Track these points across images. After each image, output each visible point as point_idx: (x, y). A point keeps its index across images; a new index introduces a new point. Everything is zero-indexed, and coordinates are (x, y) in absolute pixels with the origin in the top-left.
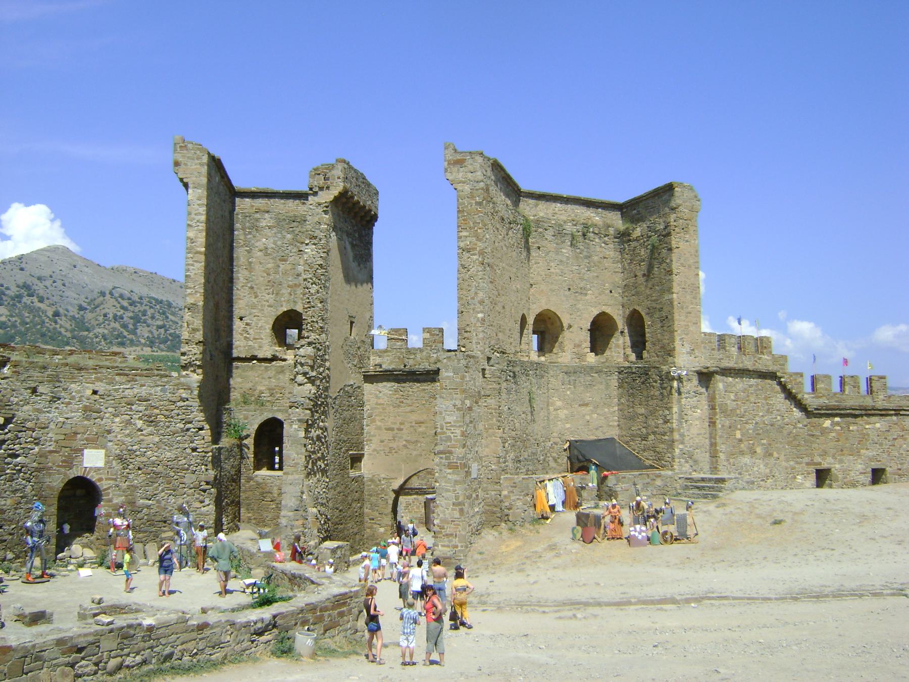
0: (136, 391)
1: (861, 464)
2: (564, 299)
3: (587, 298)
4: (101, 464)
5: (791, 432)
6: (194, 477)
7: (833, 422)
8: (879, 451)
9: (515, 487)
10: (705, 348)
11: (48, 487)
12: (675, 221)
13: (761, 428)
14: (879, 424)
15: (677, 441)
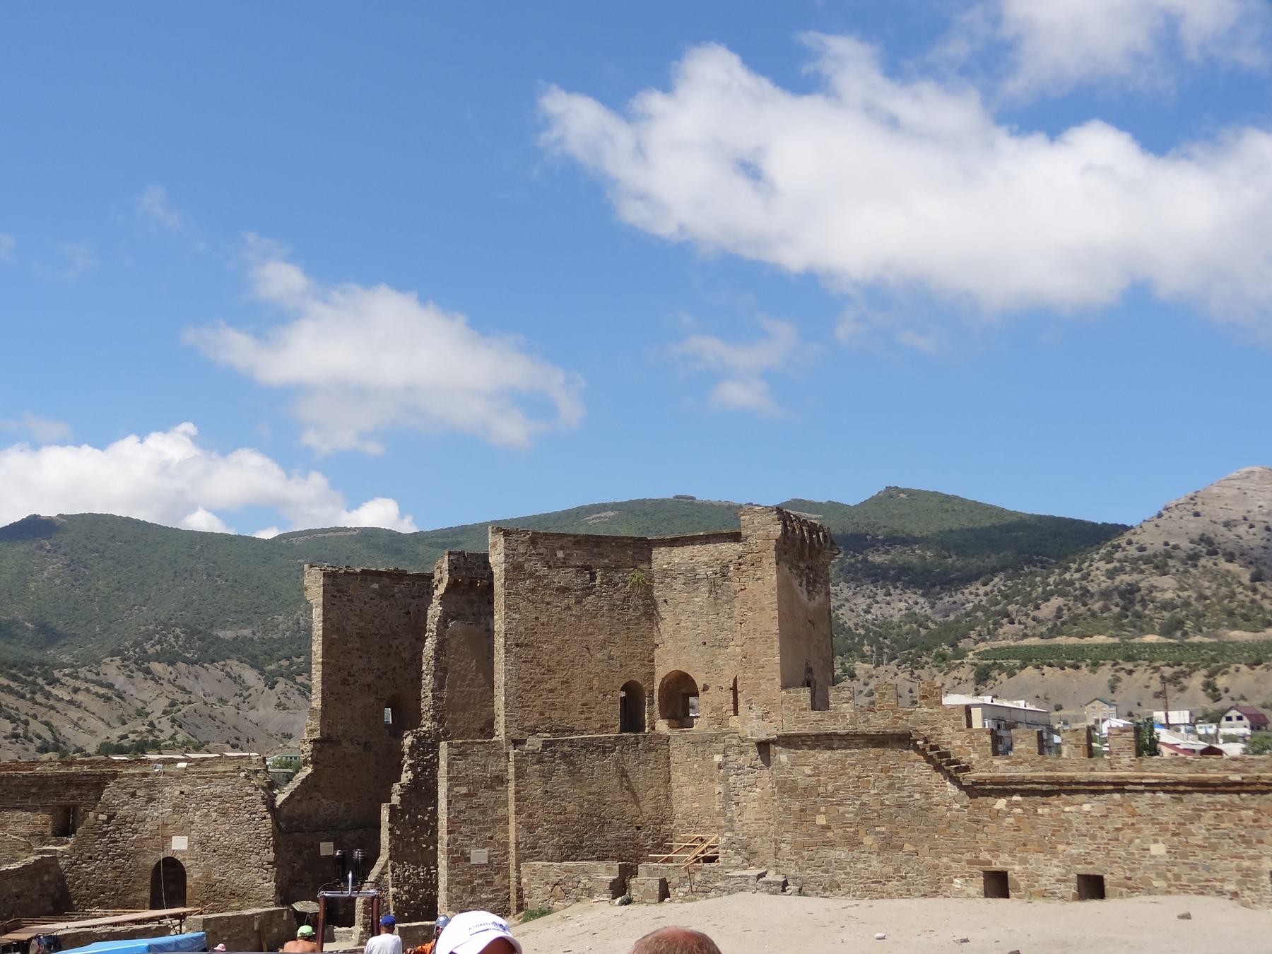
0: (212, 790)
1: (1059, 866)
2: (697, 655)
3: (728, 650)
4: (185, 847)
5: (944, 816)
6: (258, 857)
7: (1009, 801)
8: (1091, 848)
9: (535, 874)
10: (787, 709)
11: (143, 864)
12: (739, 558)
13: (876, 811)
14: (1089, 806)
15: (722, 827)
